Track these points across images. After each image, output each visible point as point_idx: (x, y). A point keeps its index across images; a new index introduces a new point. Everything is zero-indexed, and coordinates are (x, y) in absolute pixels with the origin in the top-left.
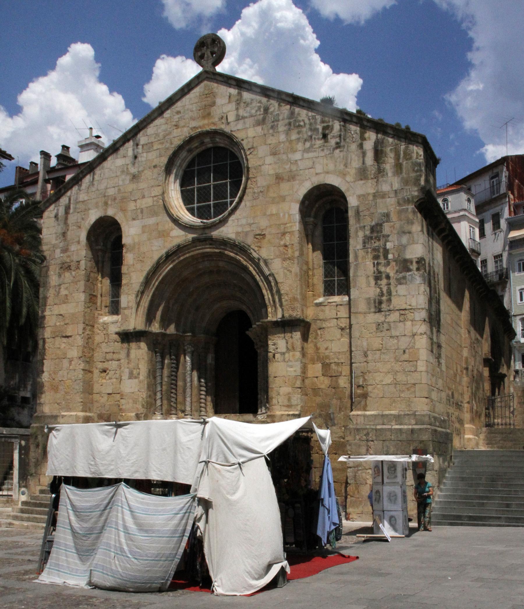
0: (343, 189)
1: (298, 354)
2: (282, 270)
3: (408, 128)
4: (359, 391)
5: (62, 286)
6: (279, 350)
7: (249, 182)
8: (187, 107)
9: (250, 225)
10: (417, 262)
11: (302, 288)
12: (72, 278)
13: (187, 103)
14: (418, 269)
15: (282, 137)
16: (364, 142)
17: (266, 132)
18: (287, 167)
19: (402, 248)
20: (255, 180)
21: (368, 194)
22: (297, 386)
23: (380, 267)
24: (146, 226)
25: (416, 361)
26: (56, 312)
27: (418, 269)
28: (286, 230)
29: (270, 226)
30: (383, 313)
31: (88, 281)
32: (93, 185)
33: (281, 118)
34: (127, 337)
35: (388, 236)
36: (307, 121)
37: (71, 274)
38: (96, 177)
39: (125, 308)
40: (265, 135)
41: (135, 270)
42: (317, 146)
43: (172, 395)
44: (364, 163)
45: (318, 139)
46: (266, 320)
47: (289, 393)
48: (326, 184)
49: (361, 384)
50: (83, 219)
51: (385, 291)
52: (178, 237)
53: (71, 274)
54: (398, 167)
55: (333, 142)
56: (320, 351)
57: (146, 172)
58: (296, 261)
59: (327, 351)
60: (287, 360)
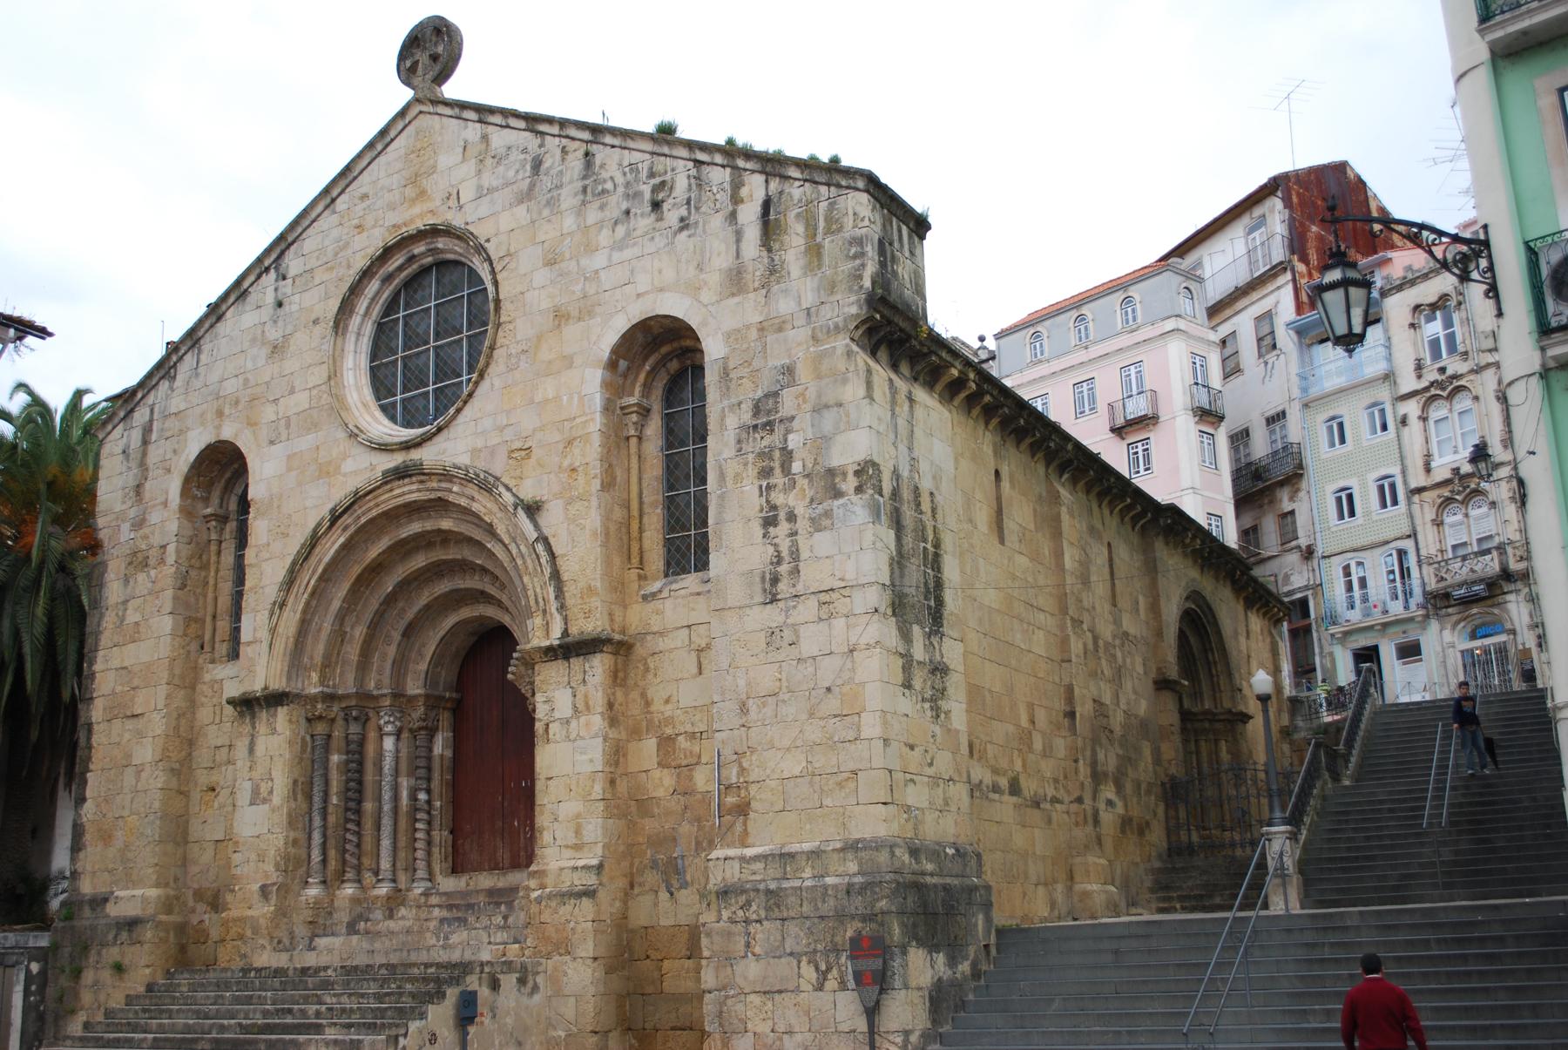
1: (597, 721)
3: (835, 160)
6: (557, 715)
7: (500, 333)
9: (502, 429)
10: (857, 473)
11: (608, 562)
13: (382, 174)
14: (859, 489)
15: (569, 222)
19: (822, 443)
20: (511, 327)
21: (748, 327)
26: (116, 663)
29: (542, 428)
30: (781, 604)
31: (183, 587)
32: (197, 375)
33: (566, 179)
34: (247, 705)
35: (793, 418)
36: (620, 180)
37: (149, 576)
38: (203, 357)
39: (249, 644)
40: (533, 222)
41: (271, 552)
43: (349, 836)
44: (738, 256)
45: (642, 215)
46: (528, 646)
47: (578, 816)
49: (734, 780)
51: (785, 553)
52: (355, 473)
53: (149, 576)
54: (814, 251)
55: (672, 216)
56: (653, 708)
57: (297, 335)
58: (594, 502)
59: (669, 707)
60: (572, 736)
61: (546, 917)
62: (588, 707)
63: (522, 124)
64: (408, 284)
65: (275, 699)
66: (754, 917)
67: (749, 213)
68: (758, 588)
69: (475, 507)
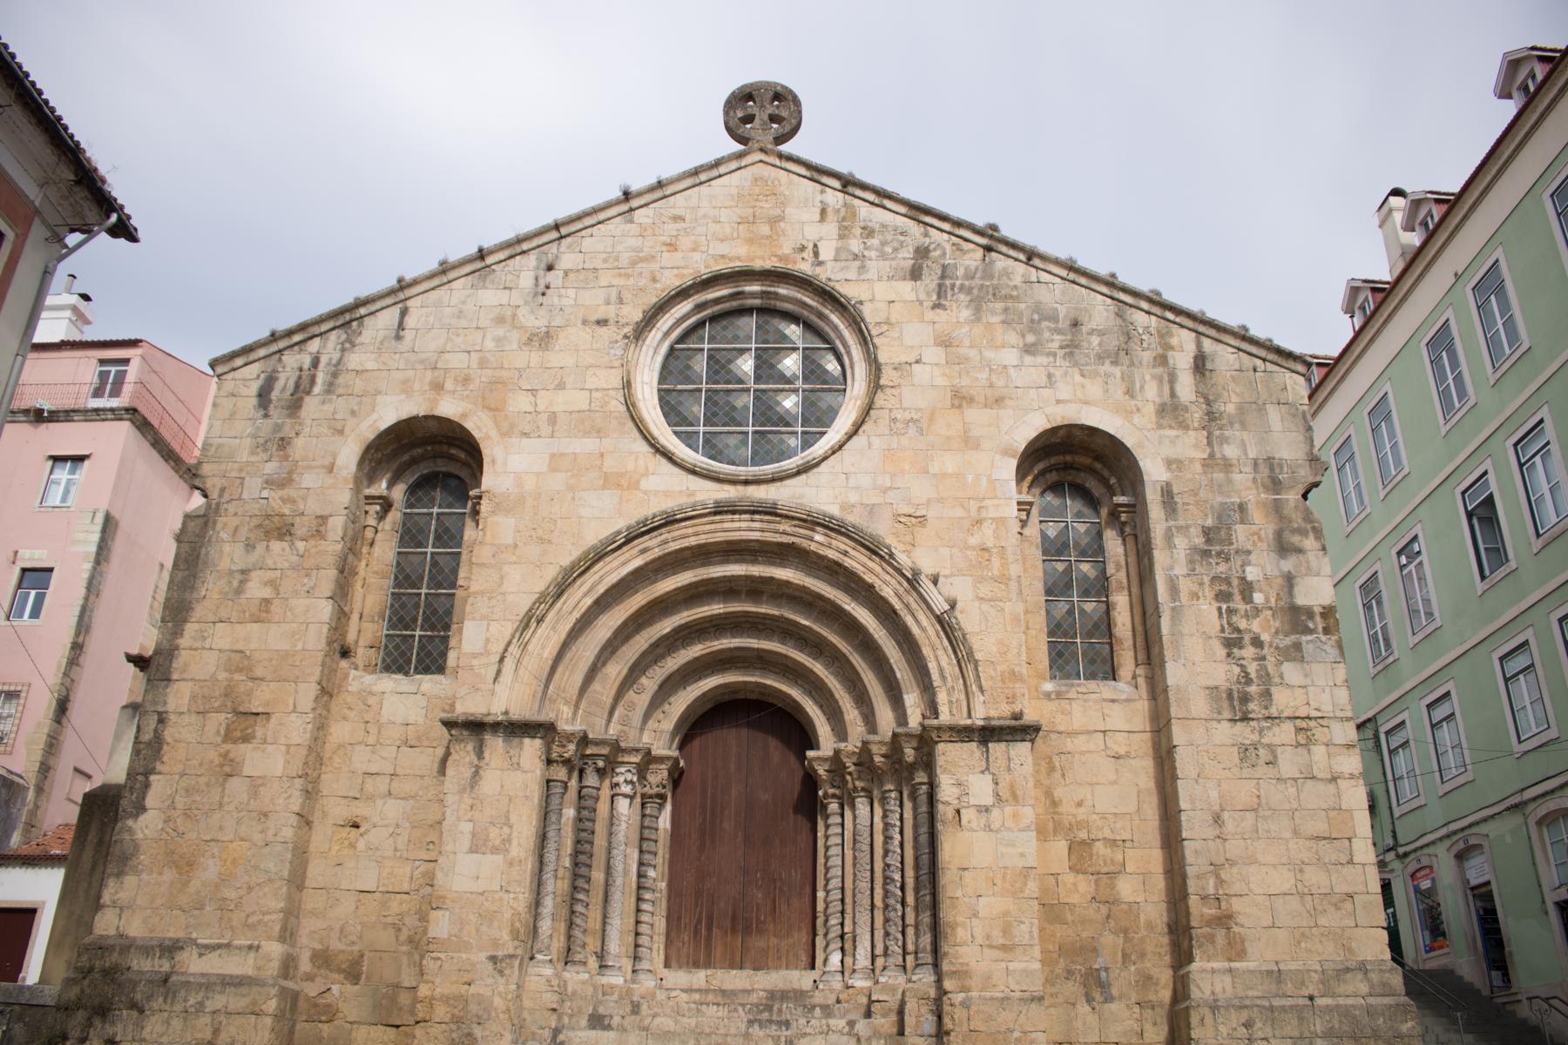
0: (1129, 442)
2: (977, 604)
4: (1209, 911)
5: (254, 575)
8: (701, 212)
9: (885, 491)
12: (295, 559)
14: (1326, 631)
15: (966, 314)
16: (1170, 353)
17: (922, 296)
18: (984, 375)
21: (1191, 460)
22: (1027, 893)
23: (1235, 619)
24: (563, 455)
25: (1350, 839)
27: (1326, 631)
28: (984, 514)
29: (940, 500)
32: (398, 338)
35: (1249, 552)
38: (410, 321)
42: (1056, 345)
45: (1059, 331)
46: (935, 722)
47: (1006, 913)
48: (1083, 427)
49: (1211, 891)
50: (353, 413)
51: (1253, 675)
52: (666, 494)
57: (572, 330)
59: (1081, 810)
60: (995, 826)
62: (1015, 797)
63: (903, 210)
64: (713, 319)
65: (516, 729)
66: (1260, 1034)
67: (1183, 360)
68: (1225, 704)
69: (848, 562)
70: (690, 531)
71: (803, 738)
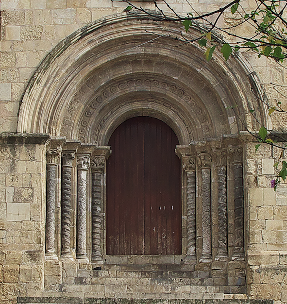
61: (264, 280)
70: (115, 30)
71: (173, 137)
